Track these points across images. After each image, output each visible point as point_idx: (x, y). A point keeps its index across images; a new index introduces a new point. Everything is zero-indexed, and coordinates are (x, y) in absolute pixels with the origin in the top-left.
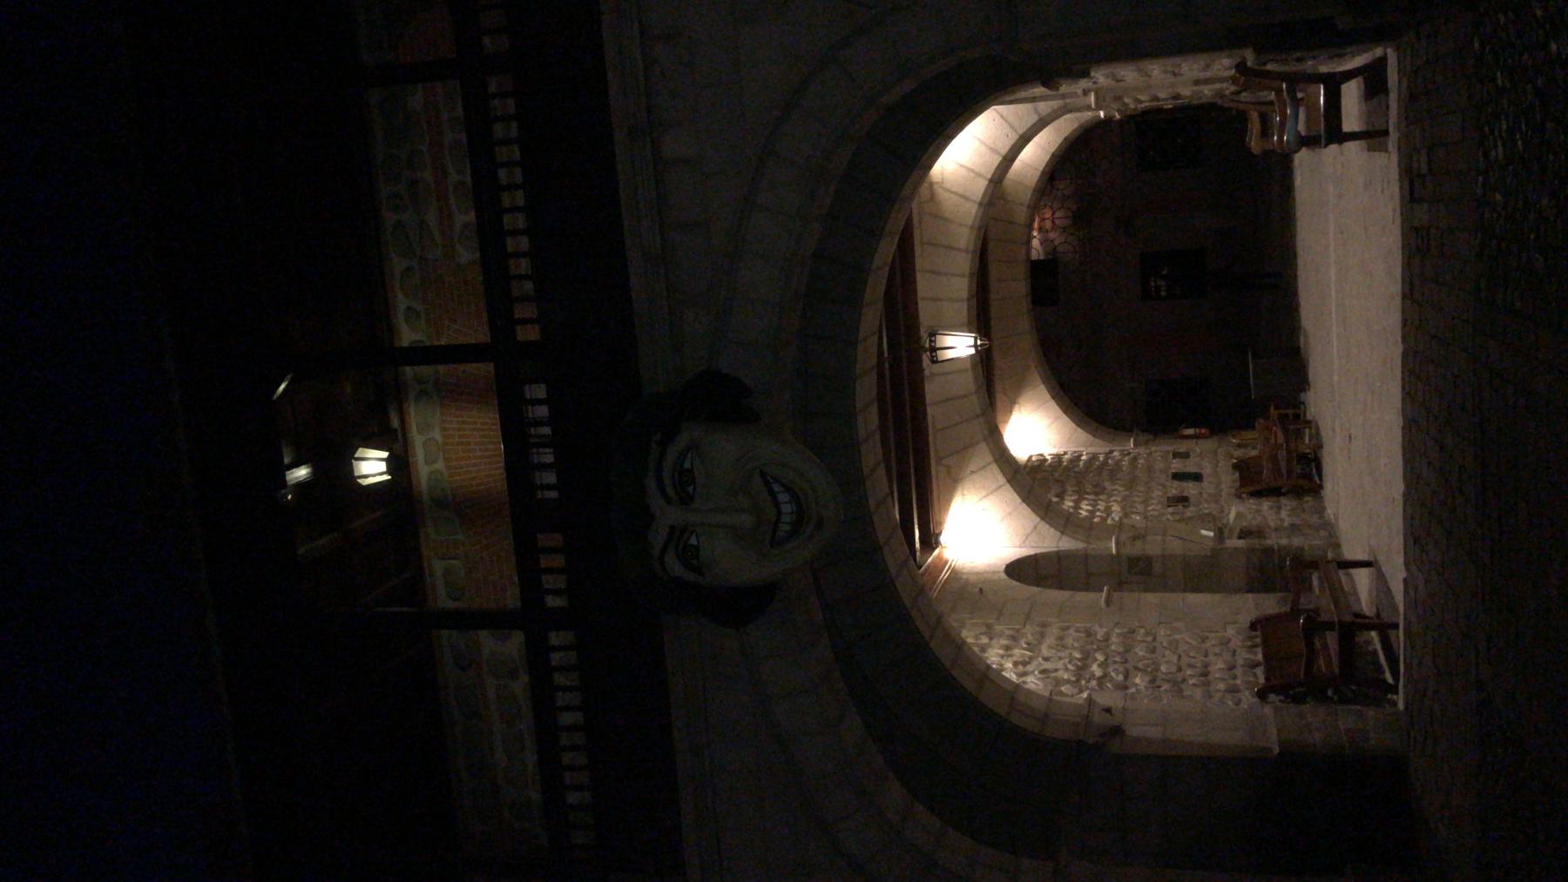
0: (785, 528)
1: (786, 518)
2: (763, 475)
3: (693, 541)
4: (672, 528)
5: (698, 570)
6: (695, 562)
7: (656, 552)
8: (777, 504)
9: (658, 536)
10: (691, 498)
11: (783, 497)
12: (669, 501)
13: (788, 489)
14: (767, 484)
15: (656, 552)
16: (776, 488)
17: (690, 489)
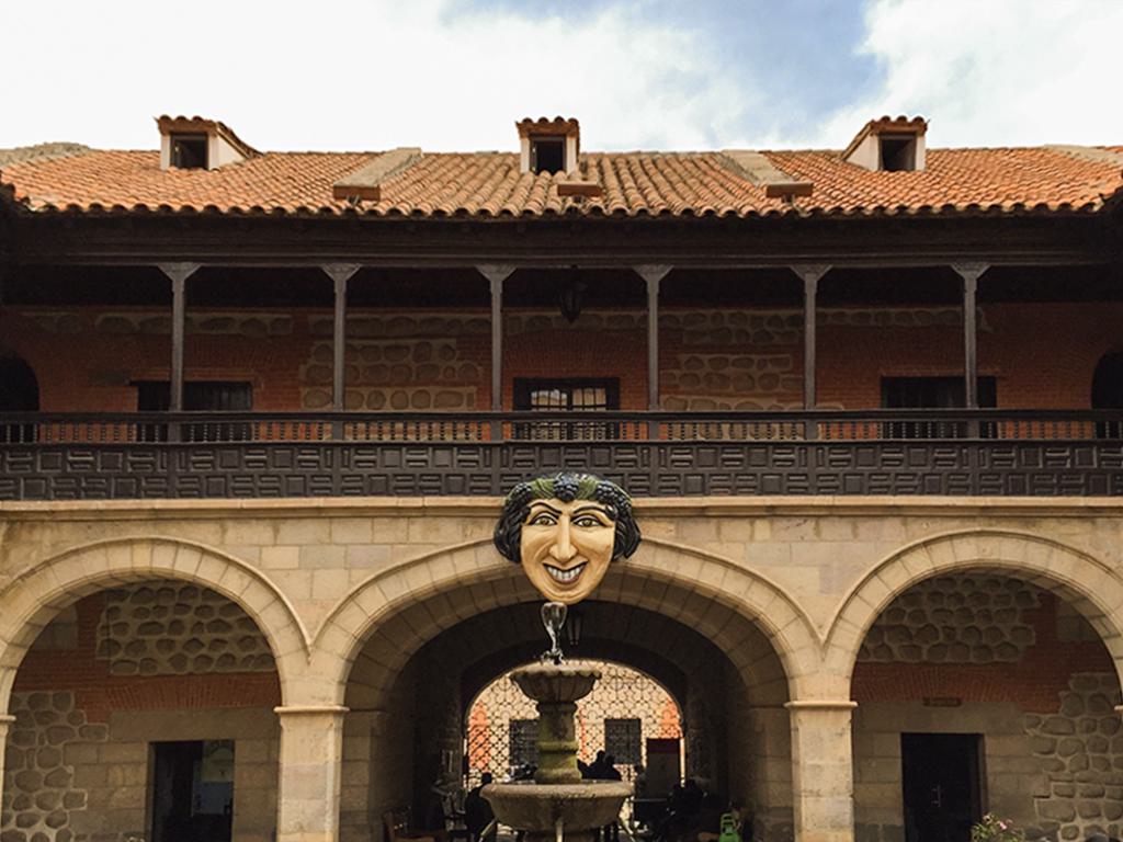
0: (555, 572)
1: (560, 573)
2: (584, 564)
3: (551, 522)
4: (560, 512)
5: (532, 523)
6: (538, 522)
7: (546, 501)
8: (569, 570)
9: (554, 503)
10: (576, 523)
11: (572, 573)
12: (575, 512)
13: (577, 577)
14: (578, 566)
15: (546, 501)
16: (578, 570)
17: (580, 523)
